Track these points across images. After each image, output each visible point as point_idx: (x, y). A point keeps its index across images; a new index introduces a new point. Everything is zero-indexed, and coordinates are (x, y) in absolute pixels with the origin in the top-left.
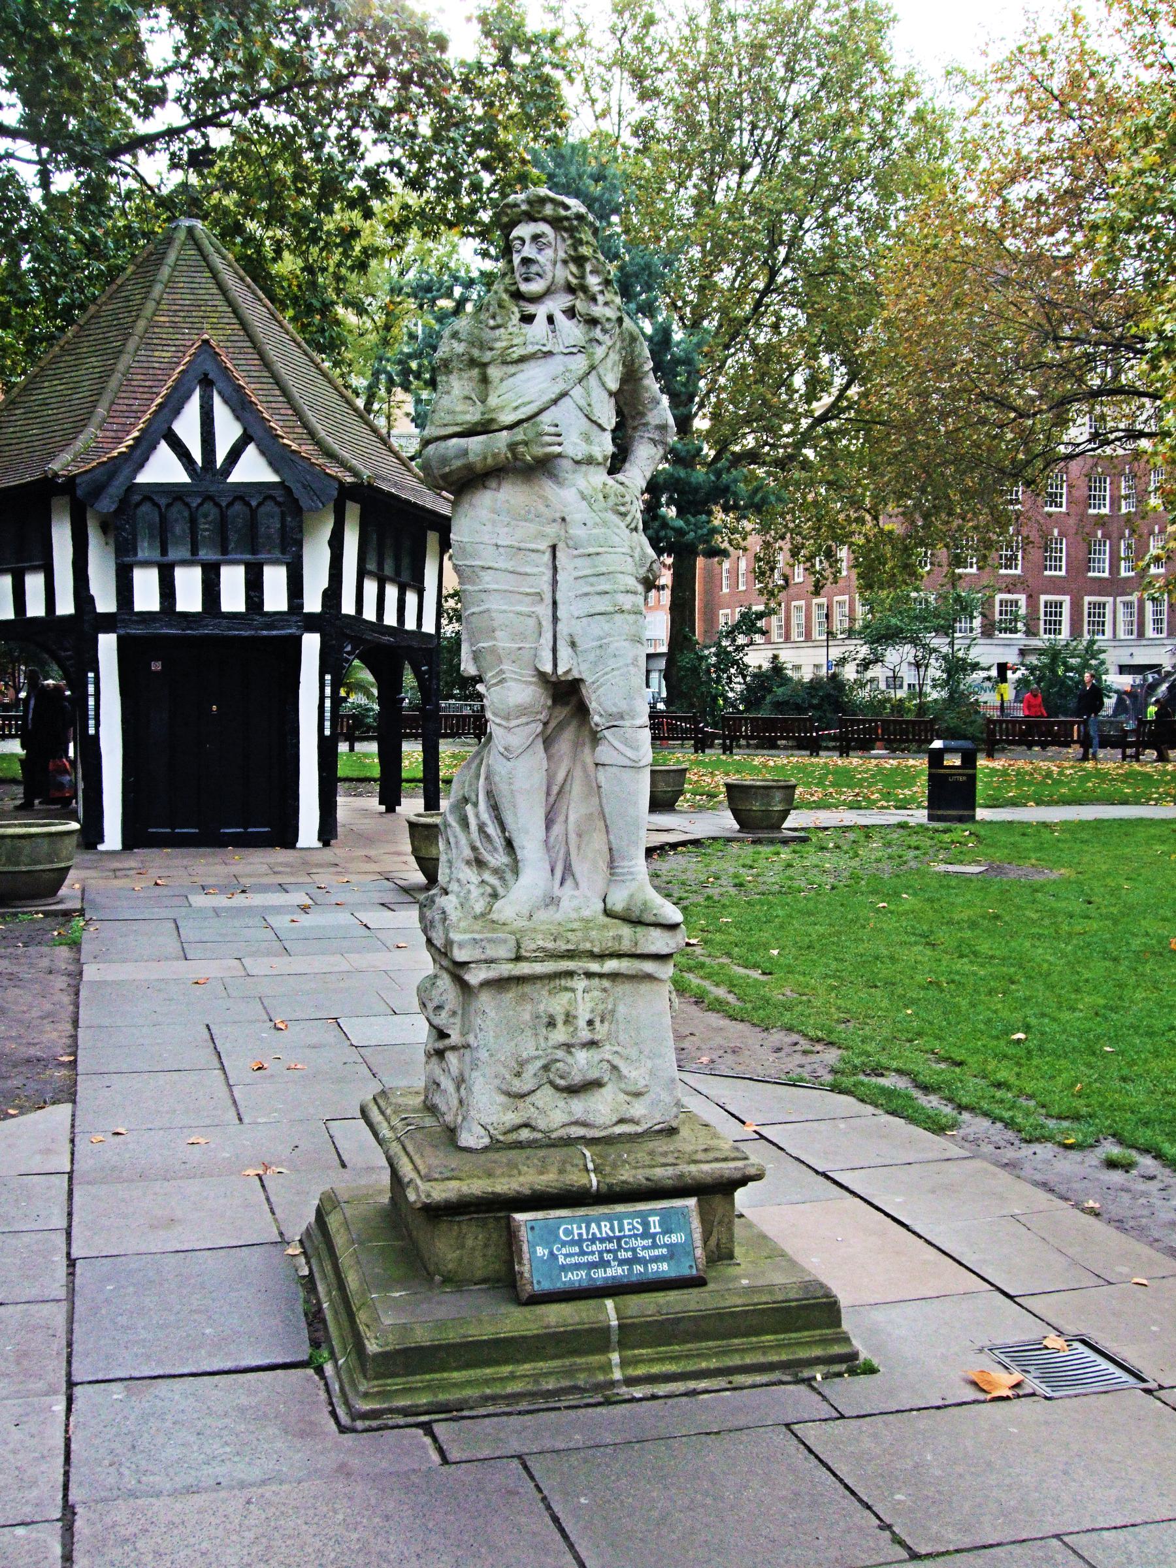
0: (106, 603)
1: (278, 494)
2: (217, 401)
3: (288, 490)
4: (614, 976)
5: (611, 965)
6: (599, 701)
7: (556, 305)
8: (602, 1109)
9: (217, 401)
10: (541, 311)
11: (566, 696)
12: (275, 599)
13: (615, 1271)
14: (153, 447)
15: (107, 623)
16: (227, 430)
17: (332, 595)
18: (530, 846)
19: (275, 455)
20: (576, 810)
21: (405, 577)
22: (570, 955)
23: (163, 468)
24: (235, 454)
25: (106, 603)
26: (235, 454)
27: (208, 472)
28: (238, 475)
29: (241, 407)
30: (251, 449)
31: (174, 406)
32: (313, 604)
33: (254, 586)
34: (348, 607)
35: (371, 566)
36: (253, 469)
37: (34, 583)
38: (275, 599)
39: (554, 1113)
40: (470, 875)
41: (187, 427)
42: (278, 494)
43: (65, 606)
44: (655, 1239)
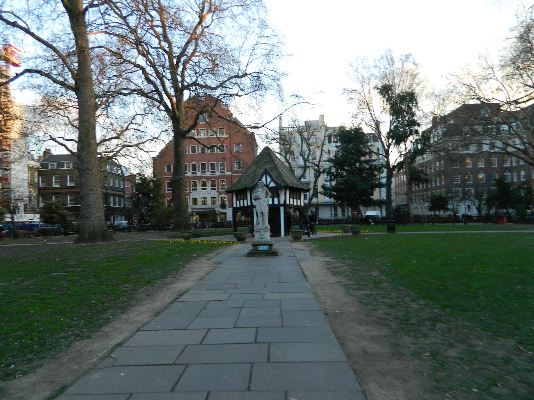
8: (263, 240)
11: (262, 213)
12: (276, 202)
16: (269, 180)
17: (285, 201)
19: (275, 183)
21: (298, 197)
24: (270, 183)
26: (270, 183)
28: (271, 186)
29: (271, 176)
31: (262, 177)
32: (282, 202)
33: (273, 201)
34: (288, 202)
35: (292, 196)
37: (245, 201)
38: (276, 202)
39: (260, 240)
43: (249, 204)
44: (265, 248)
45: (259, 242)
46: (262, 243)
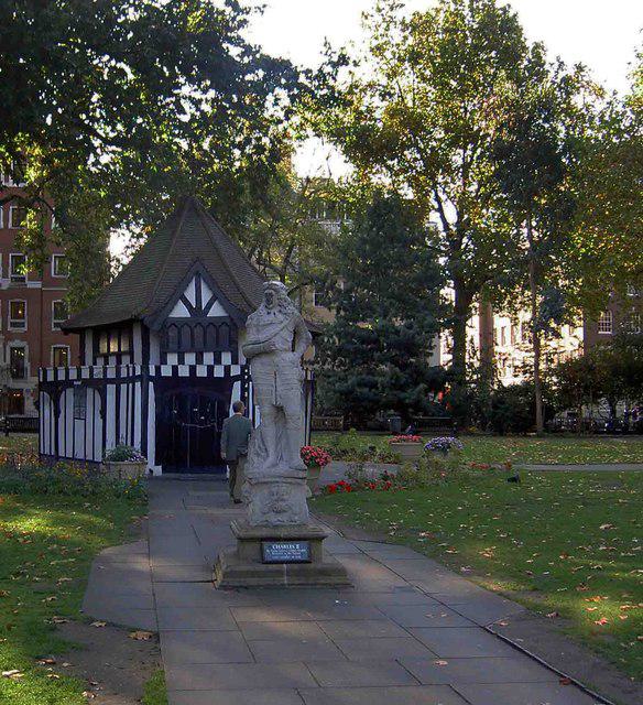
0: (152, 373)
1: (228, 321)
2: (203, 286)
3: (232, 320)
4: (290, 483)
5: (289, 480)
6: (288, 411)
7: (276, 310)
8: (284, 518)
9: (203, 286)
10: (272, 311)
13: (287, 557)
14: (176, 303)
15: (151, 379)
16: (206, 296)
18: (271, 451)
19: (225, 304)
20: (284, 441)
22: (280, 477)
23: (180, 311)
24: (209, 305)
25: (152, 373)
26: (209, 305)
27: (197, 311)
30: (216, 304)
36: (216, 311)
39: (273, 518)
40: (255, 459)
41: (190, 294)
42: (228, 321)
44: (296, 551)
45: (267, 525)
46: (282, 533)
